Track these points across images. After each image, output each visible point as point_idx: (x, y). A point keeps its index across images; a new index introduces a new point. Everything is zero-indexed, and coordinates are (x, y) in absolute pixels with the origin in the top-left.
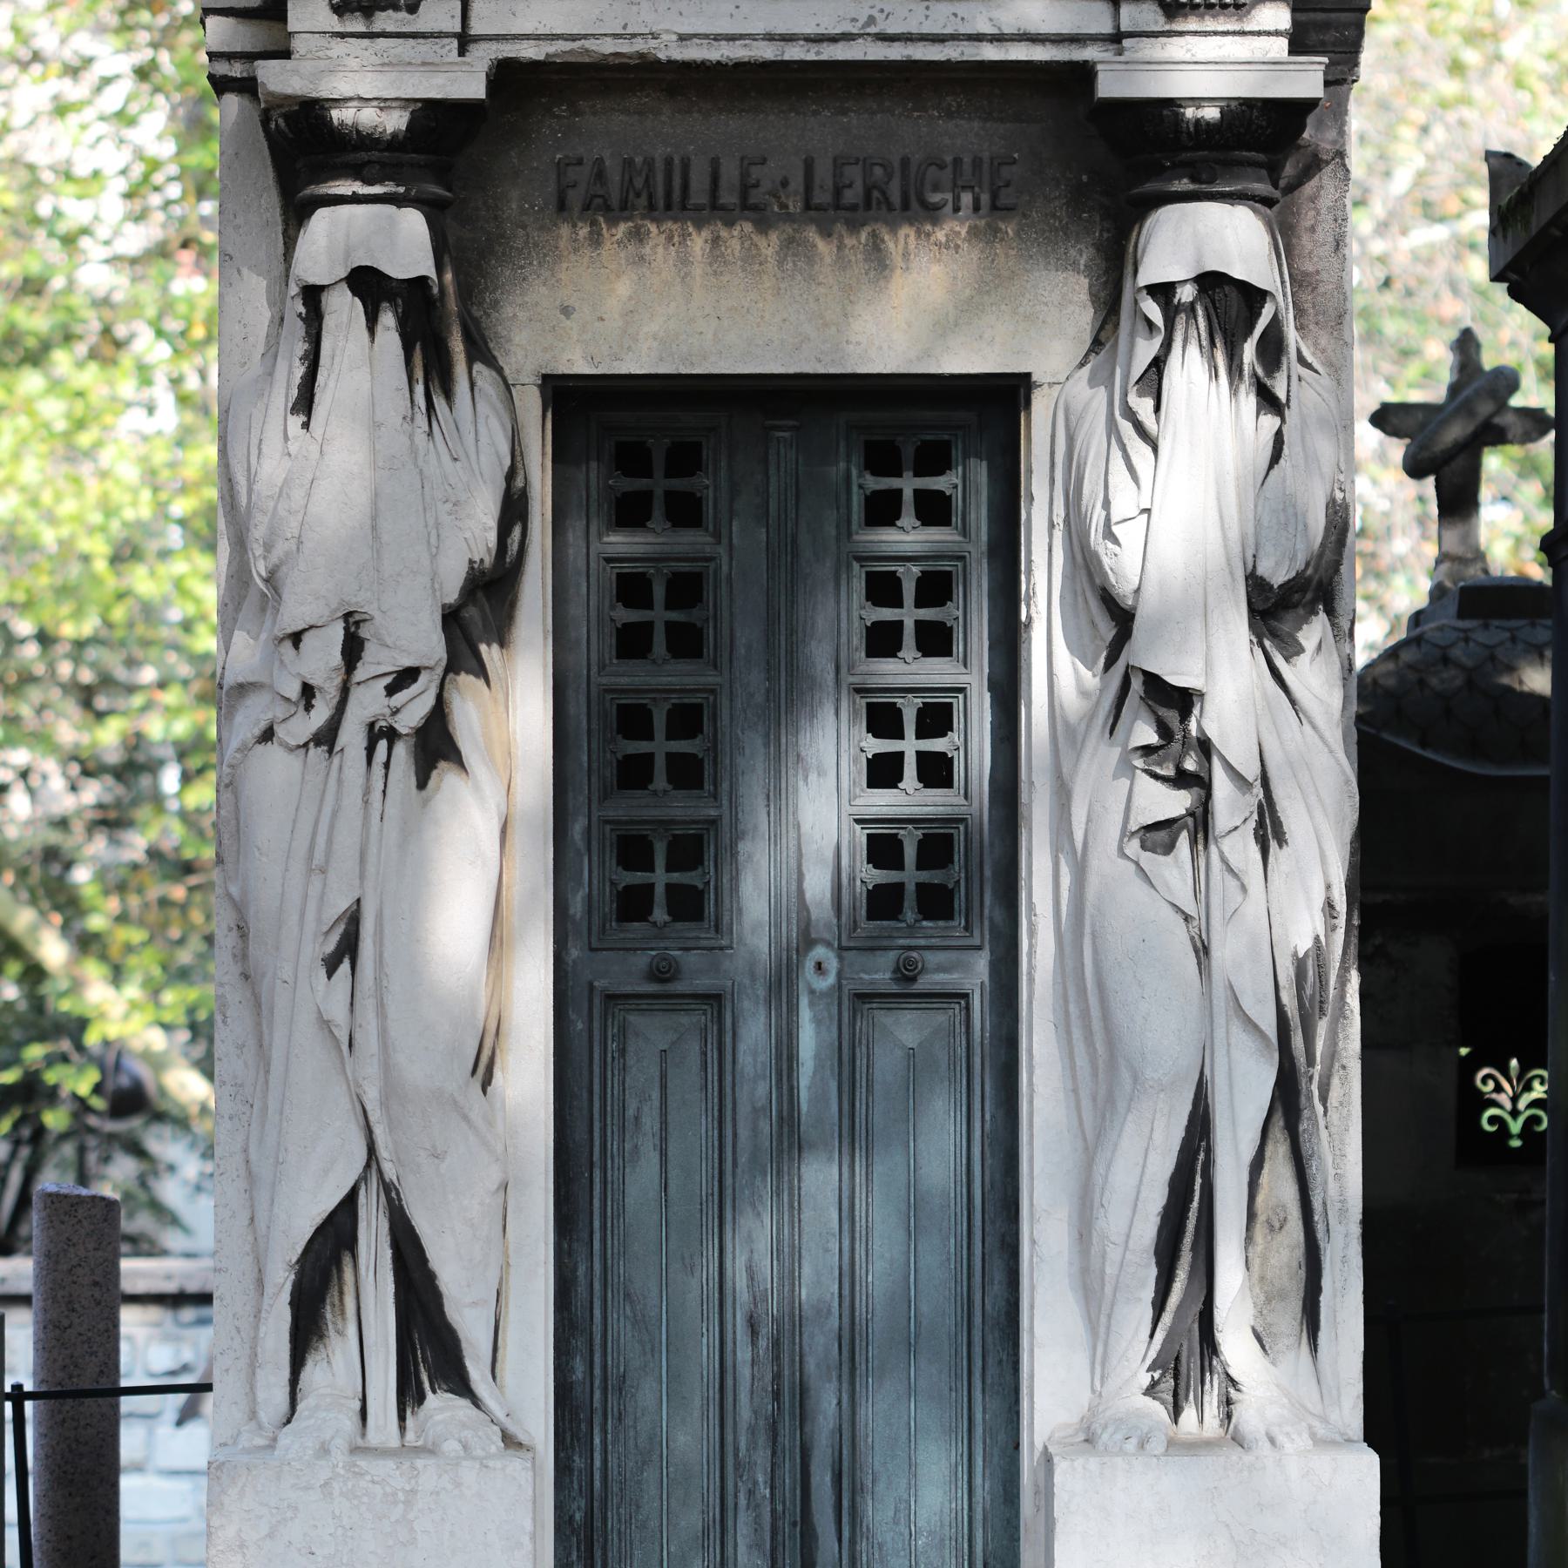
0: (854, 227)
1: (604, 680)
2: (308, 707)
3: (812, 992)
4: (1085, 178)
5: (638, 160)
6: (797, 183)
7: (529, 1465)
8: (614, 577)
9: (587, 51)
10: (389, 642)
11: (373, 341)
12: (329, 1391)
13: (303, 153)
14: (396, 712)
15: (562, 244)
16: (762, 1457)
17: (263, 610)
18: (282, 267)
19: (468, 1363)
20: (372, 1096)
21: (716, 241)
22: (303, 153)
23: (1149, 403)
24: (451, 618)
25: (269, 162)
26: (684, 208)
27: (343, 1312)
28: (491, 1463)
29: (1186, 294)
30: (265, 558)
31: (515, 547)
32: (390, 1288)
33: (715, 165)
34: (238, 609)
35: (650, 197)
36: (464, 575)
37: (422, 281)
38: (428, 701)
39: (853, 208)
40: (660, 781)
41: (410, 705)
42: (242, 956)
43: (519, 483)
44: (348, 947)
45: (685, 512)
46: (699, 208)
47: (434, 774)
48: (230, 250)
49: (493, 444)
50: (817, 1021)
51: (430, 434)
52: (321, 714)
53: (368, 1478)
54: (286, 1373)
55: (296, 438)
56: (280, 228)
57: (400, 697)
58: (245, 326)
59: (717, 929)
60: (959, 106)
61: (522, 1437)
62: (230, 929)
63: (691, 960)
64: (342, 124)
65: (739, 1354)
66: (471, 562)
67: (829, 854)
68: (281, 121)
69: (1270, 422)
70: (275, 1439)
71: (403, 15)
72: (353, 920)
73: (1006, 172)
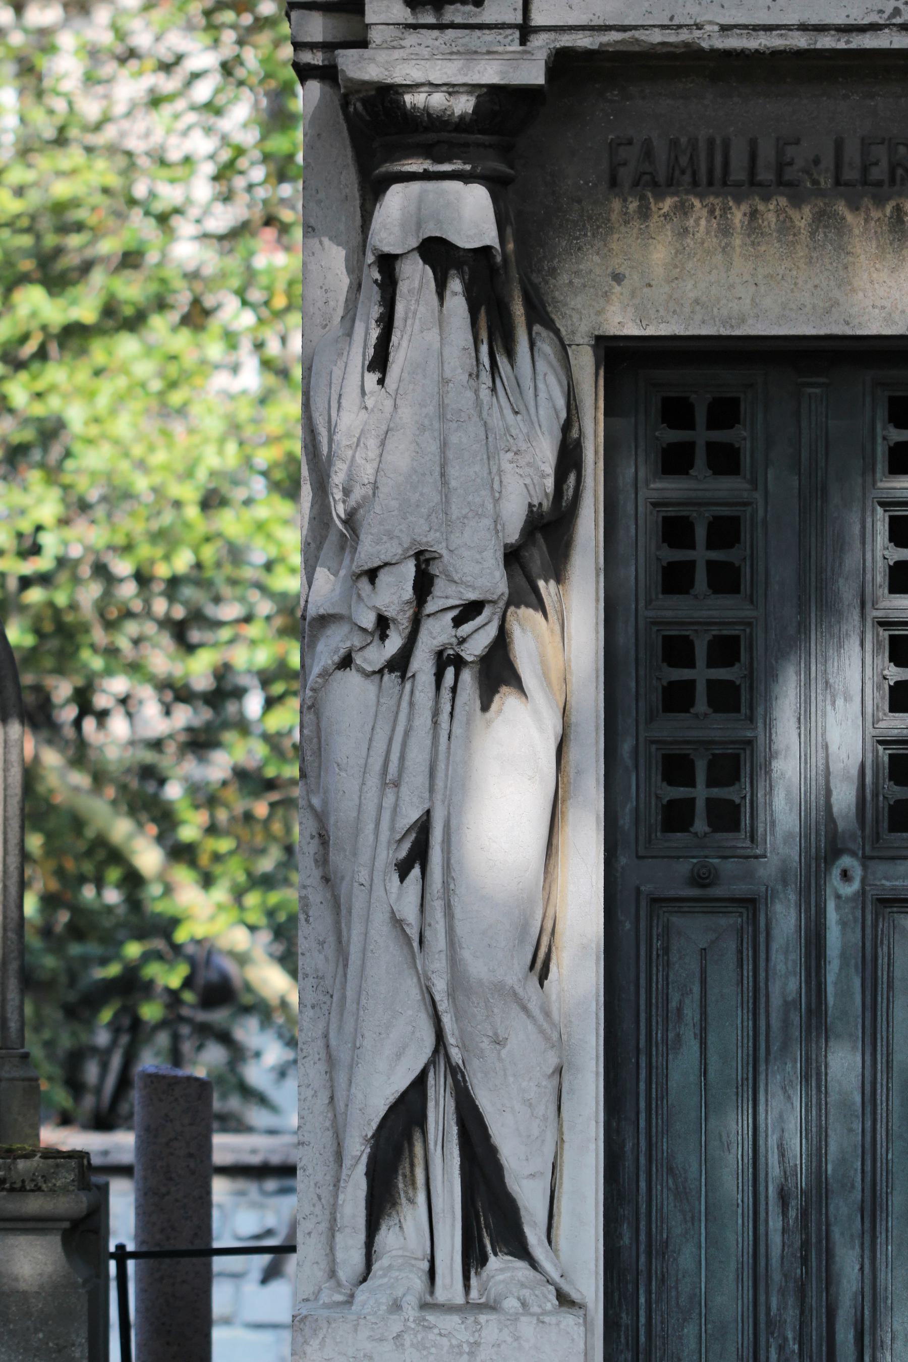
0: (880, 202)
1: (651, 614)
2: (383, 637)
3: (838, 897)
5: (683, 140)
6: (828, 161)
7: (581, 1321)
8: (660, 519)
9: (637, 40)
10: (456, 578)
11: (442, 305)
12: (400, 1253)
13: (379, 135)
14: (462, 641)
15: (614, 216)
16: (791, 1315)
17: (342, 548)
18: (359, 238)
19: (527, 1230)
20: (440, 987)
21: (754, 214)
22: (379, 135)
24: (513, 557)
25: (348, 142)
26: (725, 184)
27: (414, 1183)
28: (547, 1319)
30: (344, 502)
31: (571, 492)
32: (456, 1161)
33: (753, 145)
34: (319, 548)
35: (694, 174)
36: (524, 517)
37: (486, 250)
38: (492, 631)
39: (879, 184)
40: (701, 705)
41: (476, 636)
42: (323, 861)
43: (575, 434)
44: (417, 854)
45: (725, 461)
46: (738, 184)
47: (497, 698)
48: (312, 222)
49: (550, 399)
50: (843, 924)
51: (494, 389)
52: (394, 643)
53: (436, 1331)
54: (362, 1237)
55: (372, 393)
56: (358, 203)
59: (753, 839)
61: (575, 1296)
62: (312, 837)
63: (729, 867)
64: (414, 107)
65: (771, 1223)
66: (530, 506)
67: (854, 772)
68: (359, 106)
70: (352, 1296)
71: (470, 8)
72: (423, 827)
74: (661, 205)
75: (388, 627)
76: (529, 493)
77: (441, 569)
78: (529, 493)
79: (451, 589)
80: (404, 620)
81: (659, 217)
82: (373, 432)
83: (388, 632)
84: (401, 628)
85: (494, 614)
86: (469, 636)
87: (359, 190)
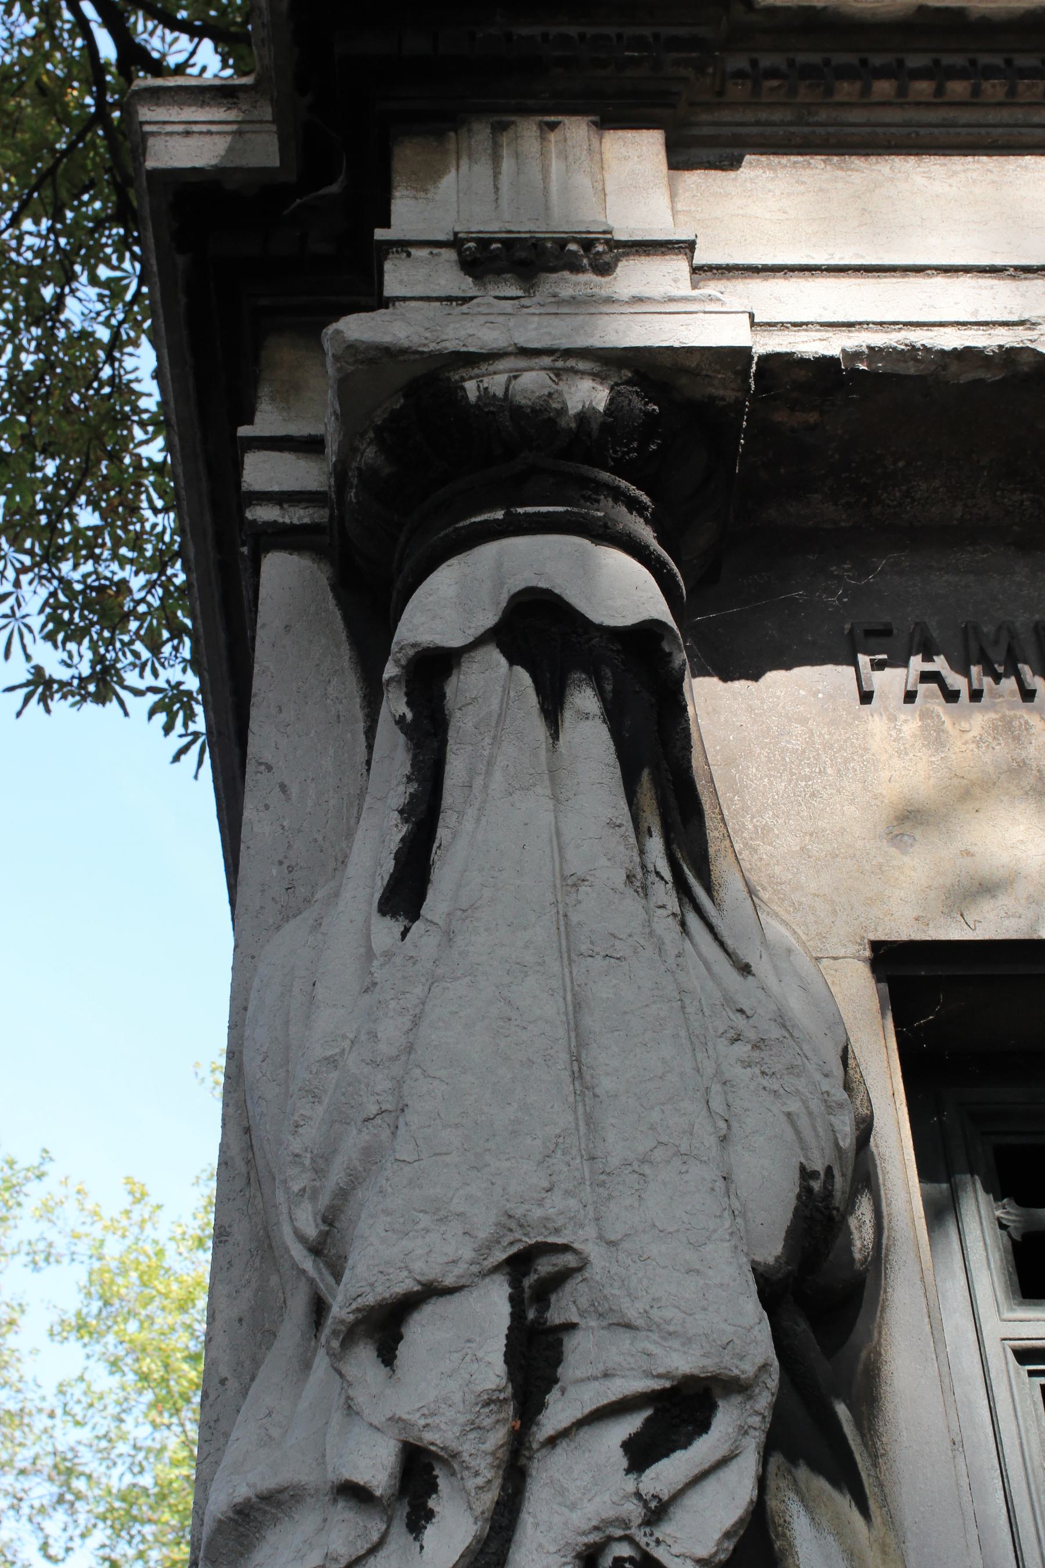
2: (419, 1519)
10: (632, 1313)
14: (657, 1512)
36: (791, 1202)
41: (695, 1499)
55: (389, 955)
57: (667, 1473)
58: (291, 869)
66: (806, 1174)
74: (965, 725)
75: (432, 1488)
76: (801, 1139)
77: (584, 1302)
78: (801, 1139)
79: (619, 1350)
80: (481, 1452)
81: (966, 743)
82: (393, 1004)
83: (431, 1503)
84: (471, 1483)
85: (744, 1431)
86: (677, 1496)
87: (362, 708)
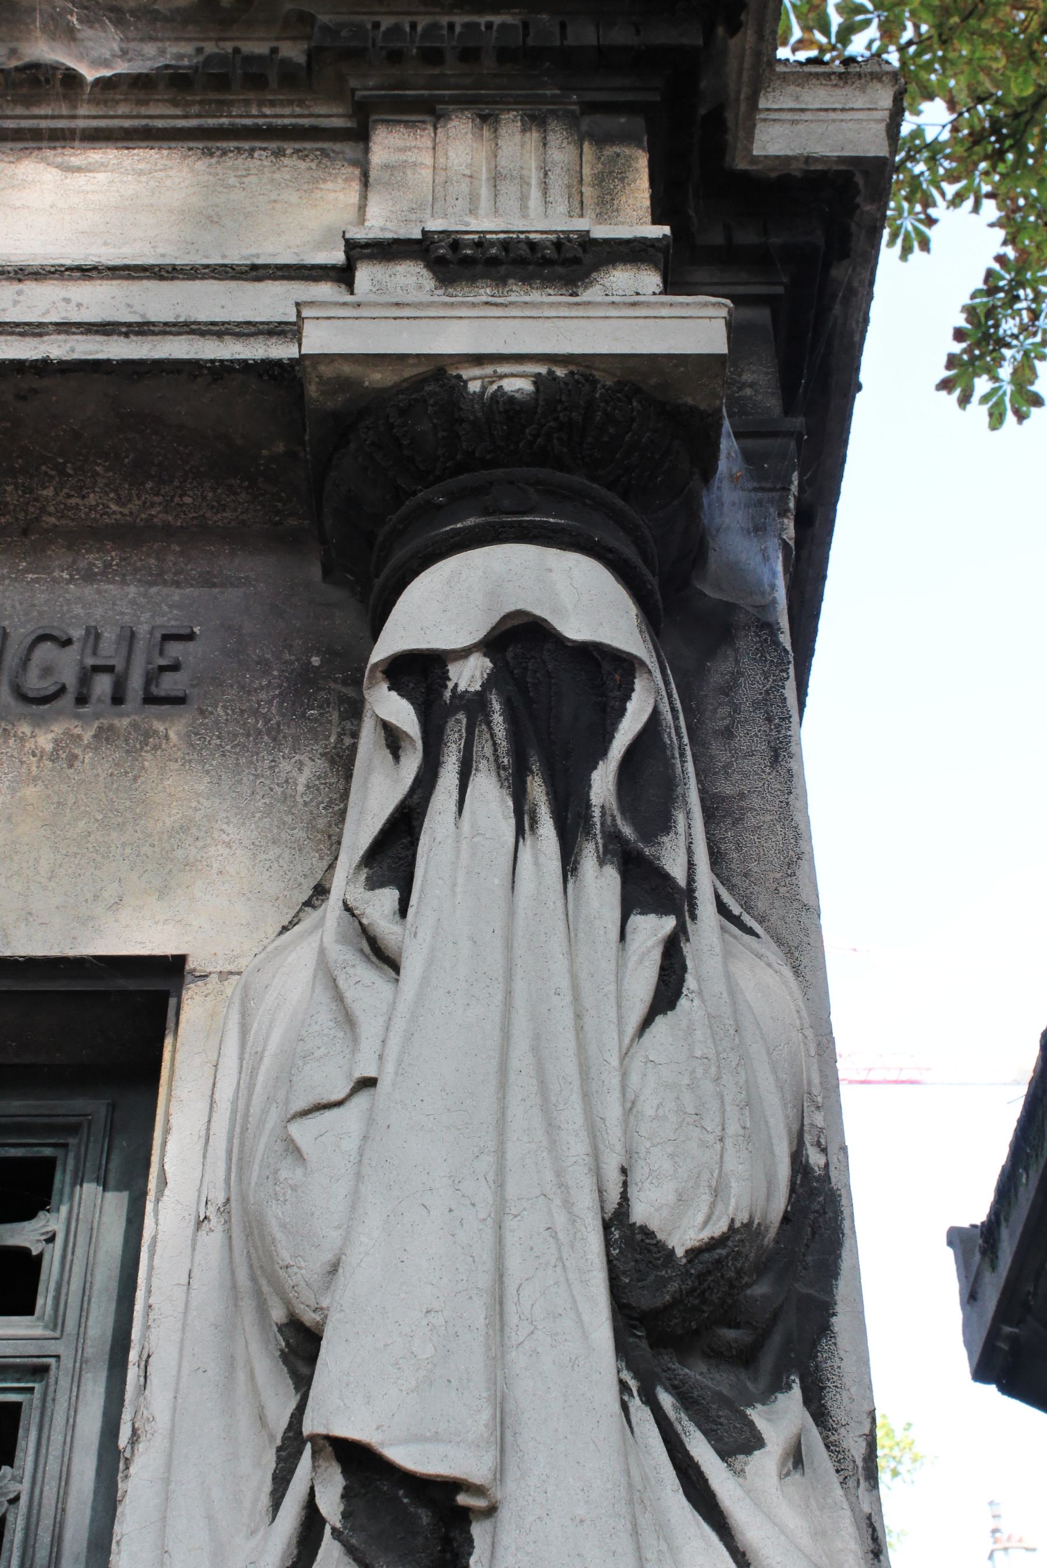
4: (316, 661)
23: (389, 896)
29: (469, 675)
60: (107, 565)
69: (652, 929)
73: (175, 650)
